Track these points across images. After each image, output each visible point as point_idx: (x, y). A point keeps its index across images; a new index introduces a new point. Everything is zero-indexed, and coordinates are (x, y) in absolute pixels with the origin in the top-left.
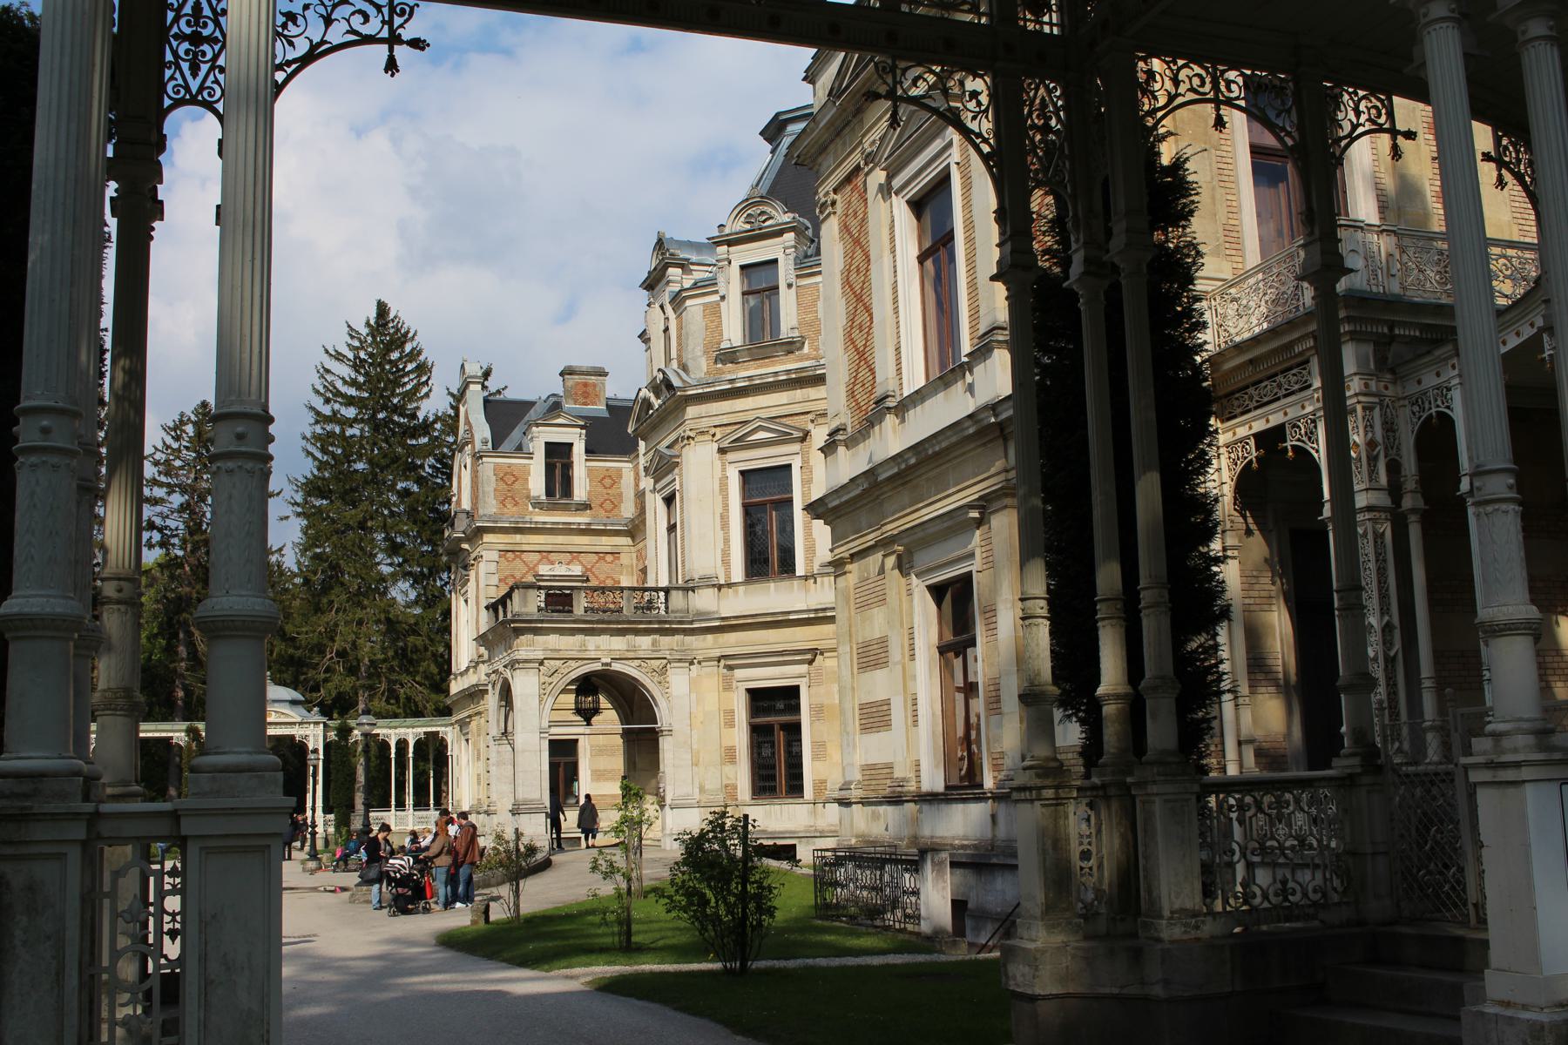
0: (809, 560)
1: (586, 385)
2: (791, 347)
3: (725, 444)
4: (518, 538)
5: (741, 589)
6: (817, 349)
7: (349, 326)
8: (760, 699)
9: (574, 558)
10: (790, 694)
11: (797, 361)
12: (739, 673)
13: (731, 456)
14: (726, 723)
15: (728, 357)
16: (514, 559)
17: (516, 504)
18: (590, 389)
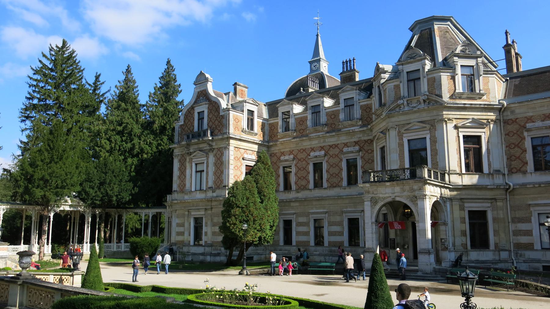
0: (489, 169)
1: (242, 91)
2: (480, 96)
3: (459, 125)
4: (239, 143)
5: (466, 176)
6: (489, 99)
7: (51, 45)
8: (472, 214)
9: (253, 153)
10: (482, 214)
11: (482, 101)
12: (466, 205)
13: (460, 130)
14: (461, 222)
15: (460, 96)
16: (237, 151)
17: (238, 130)
18: (243, 92)
